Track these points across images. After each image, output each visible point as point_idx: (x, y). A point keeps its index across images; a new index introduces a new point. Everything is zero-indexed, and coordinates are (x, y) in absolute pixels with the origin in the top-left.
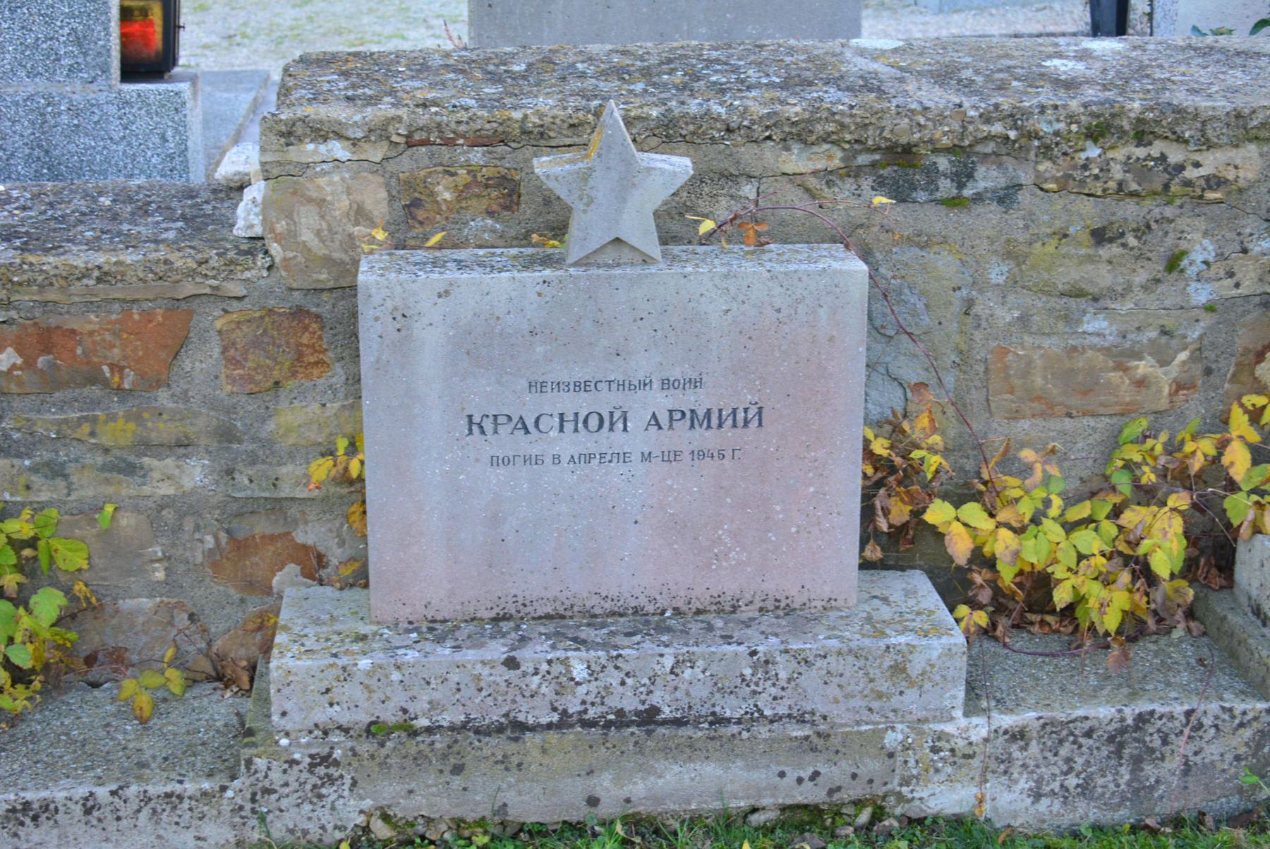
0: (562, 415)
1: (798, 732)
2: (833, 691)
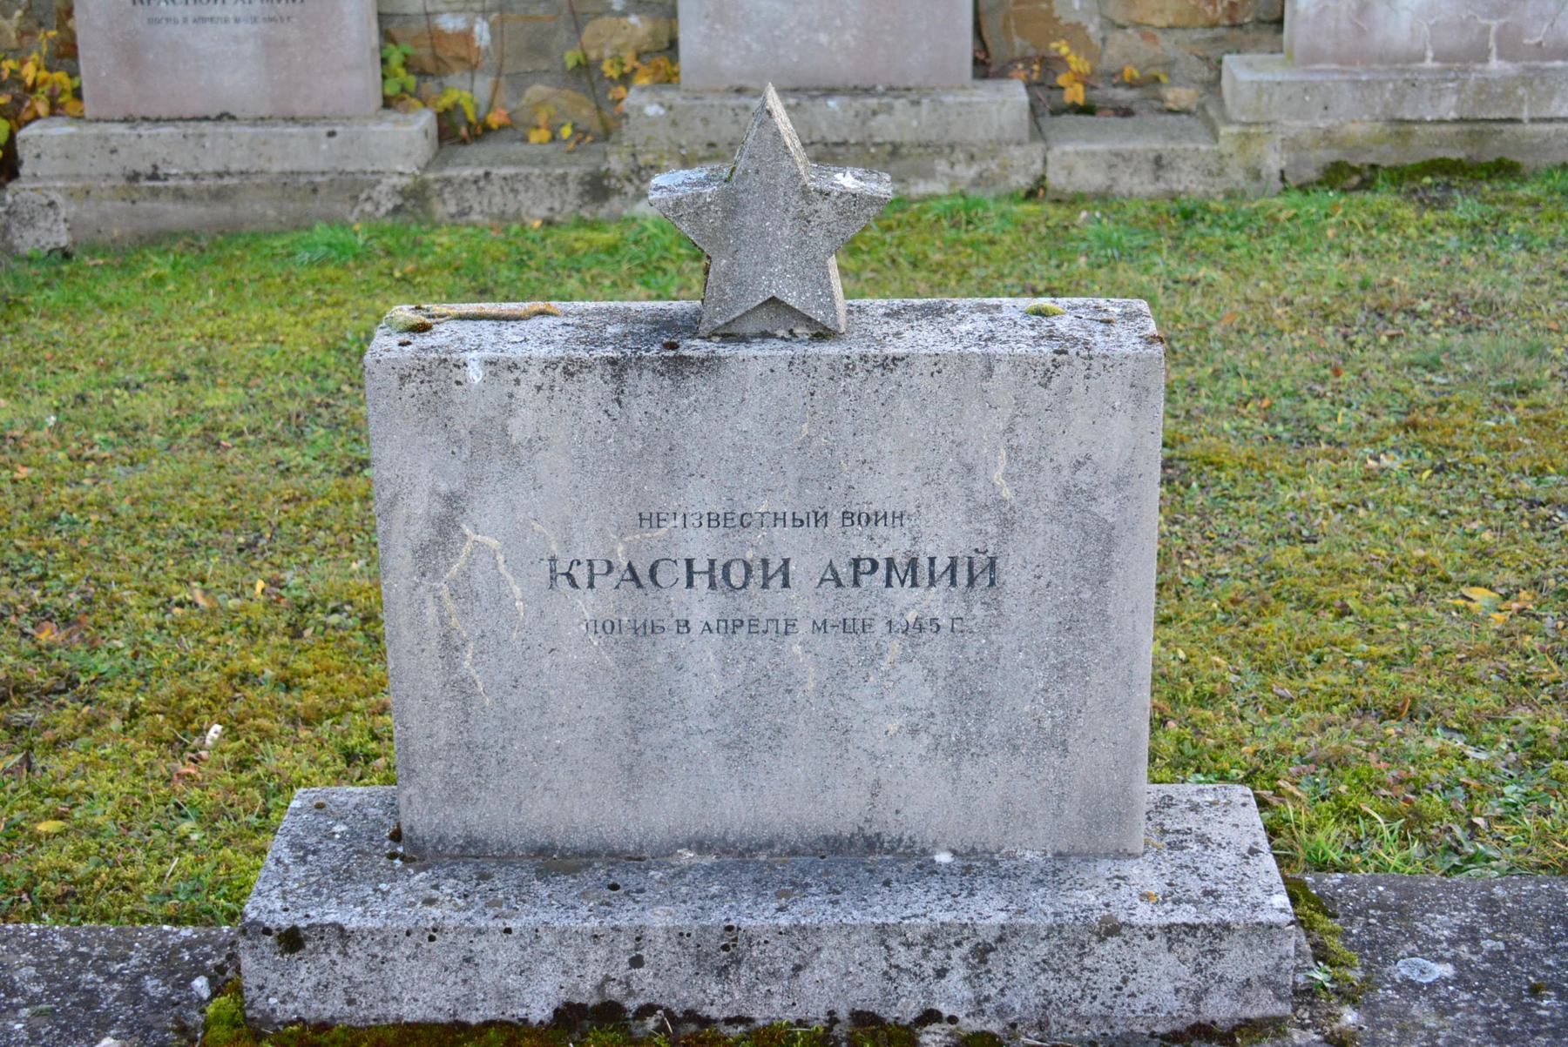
0: (689, 562)
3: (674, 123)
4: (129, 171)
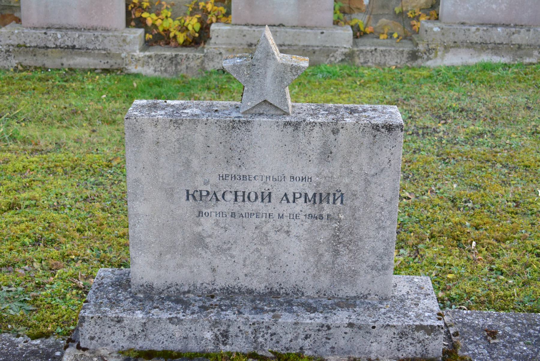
1: (103, 52)
2: (111, 44)
3: (443, 34)
4: (249, 43)
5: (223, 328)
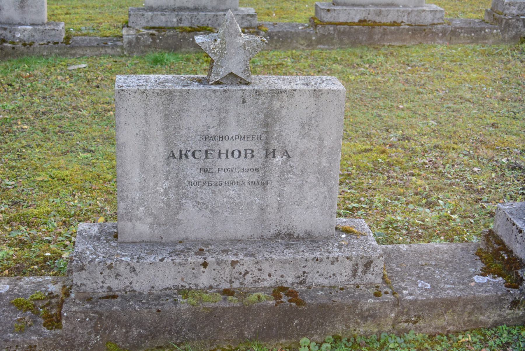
5: (180, 17)
